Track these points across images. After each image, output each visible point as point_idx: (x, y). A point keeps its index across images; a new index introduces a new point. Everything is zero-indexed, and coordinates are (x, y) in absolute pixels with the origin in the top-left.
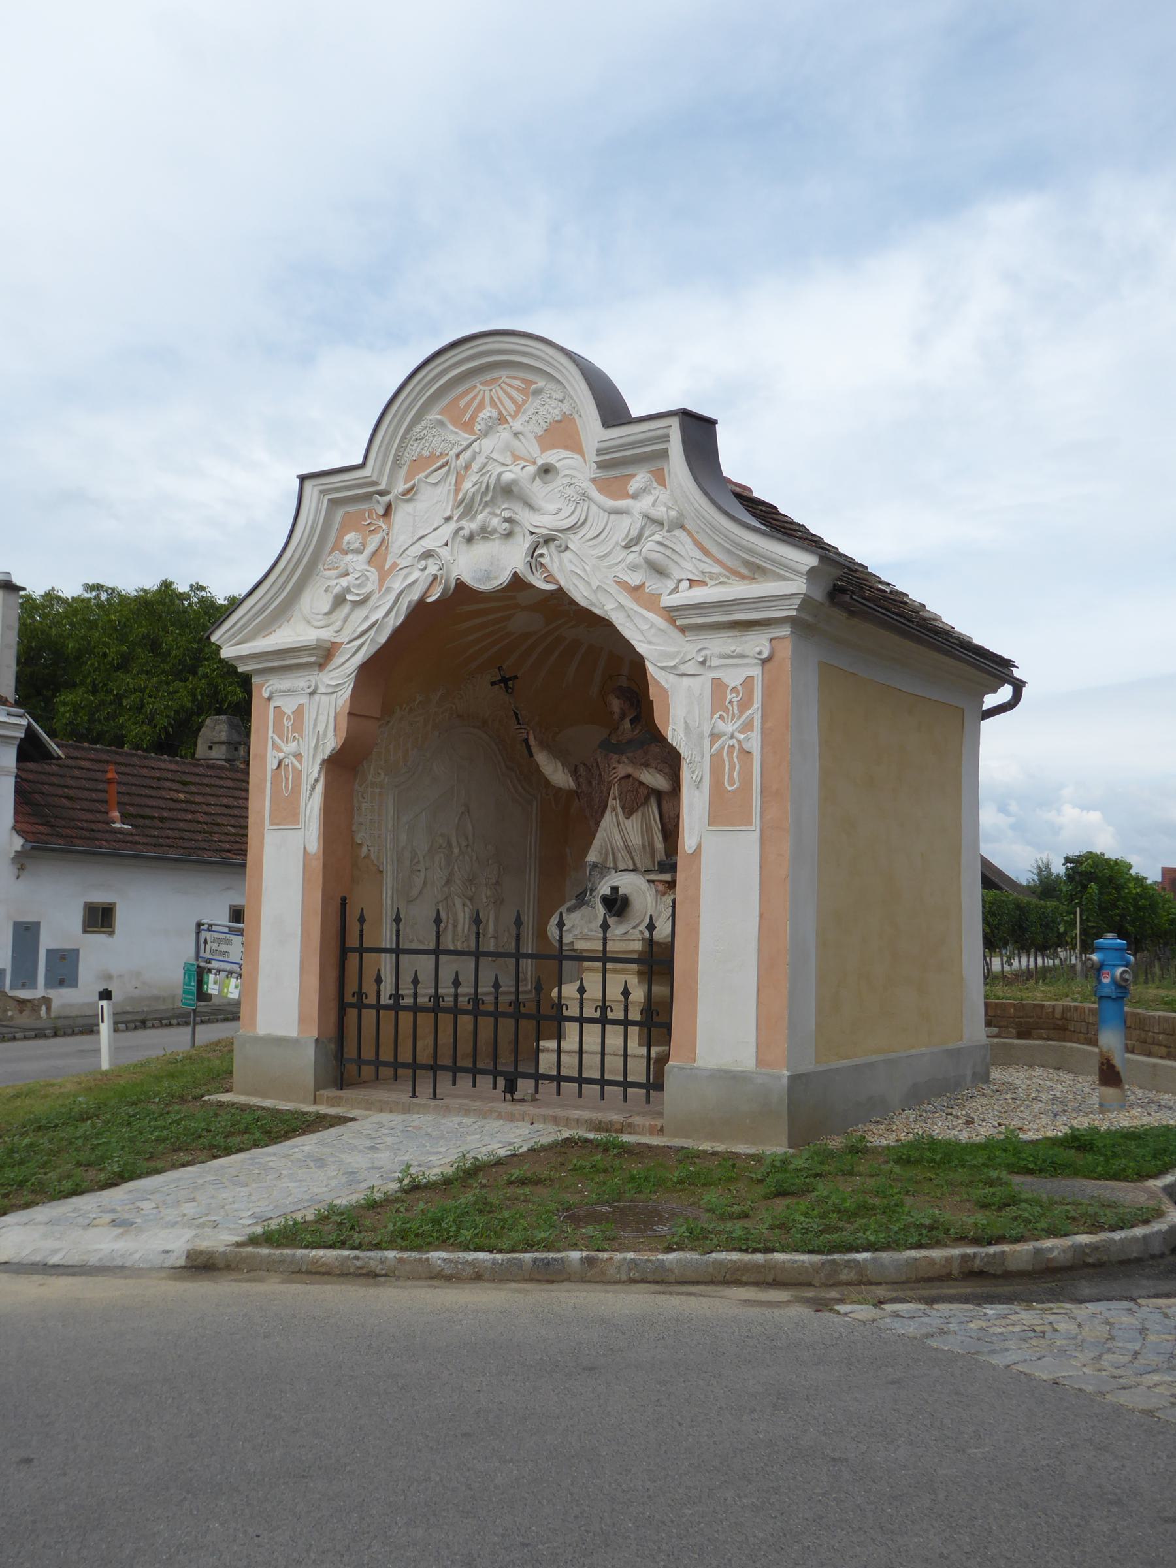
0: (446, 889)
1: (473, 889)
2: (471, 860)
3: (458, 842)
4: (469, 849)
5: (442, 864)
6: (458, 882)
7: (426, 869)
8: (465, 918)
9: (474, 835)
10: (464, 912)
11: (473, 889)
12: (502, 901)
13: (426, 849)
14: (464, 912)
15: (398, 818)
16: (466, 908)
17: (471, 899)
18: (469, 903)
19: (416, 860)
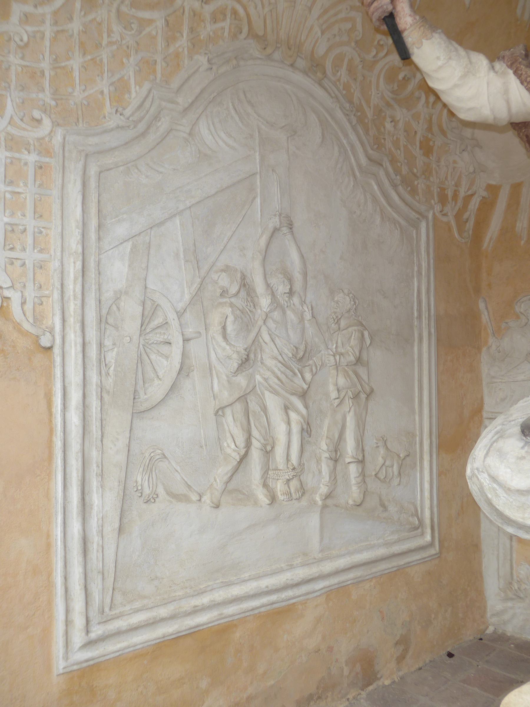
0: (242, 380)
1: (308, 376)
2: (302, 319)
3: (268, 285)
4: (296, 300)
5: (230, 328)
6: (270, 363)
7: (186, 340)
8: (289, 433)
9: (305, 275)
10: (289, 423)
11: (308, 376)
12: (369, 395)
13: (187, 297)
14: (289, 423)
15: (100, 226)
16: (293, 416)
17: (303, 395)
18: (298, 403)
19: (158, 321)
